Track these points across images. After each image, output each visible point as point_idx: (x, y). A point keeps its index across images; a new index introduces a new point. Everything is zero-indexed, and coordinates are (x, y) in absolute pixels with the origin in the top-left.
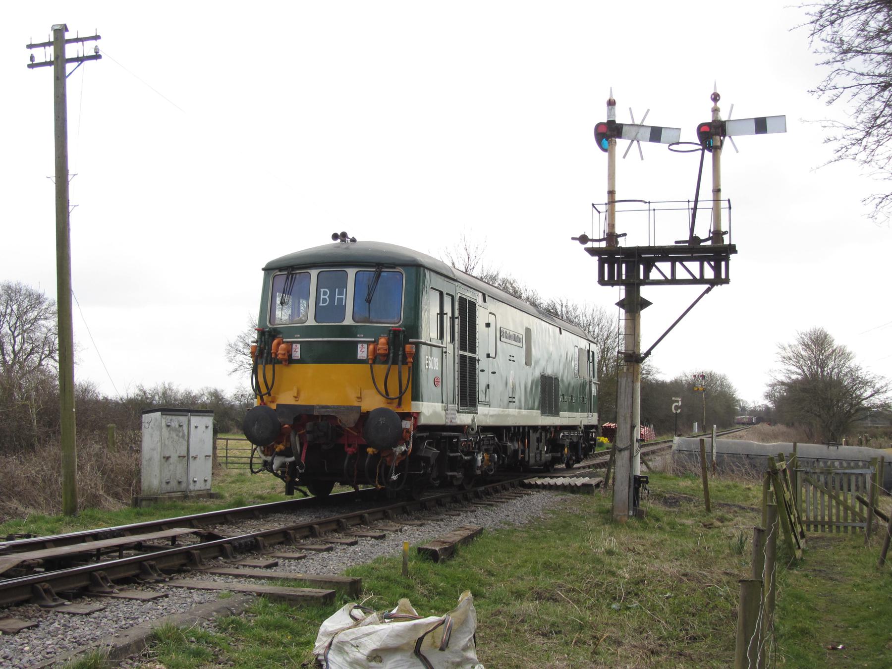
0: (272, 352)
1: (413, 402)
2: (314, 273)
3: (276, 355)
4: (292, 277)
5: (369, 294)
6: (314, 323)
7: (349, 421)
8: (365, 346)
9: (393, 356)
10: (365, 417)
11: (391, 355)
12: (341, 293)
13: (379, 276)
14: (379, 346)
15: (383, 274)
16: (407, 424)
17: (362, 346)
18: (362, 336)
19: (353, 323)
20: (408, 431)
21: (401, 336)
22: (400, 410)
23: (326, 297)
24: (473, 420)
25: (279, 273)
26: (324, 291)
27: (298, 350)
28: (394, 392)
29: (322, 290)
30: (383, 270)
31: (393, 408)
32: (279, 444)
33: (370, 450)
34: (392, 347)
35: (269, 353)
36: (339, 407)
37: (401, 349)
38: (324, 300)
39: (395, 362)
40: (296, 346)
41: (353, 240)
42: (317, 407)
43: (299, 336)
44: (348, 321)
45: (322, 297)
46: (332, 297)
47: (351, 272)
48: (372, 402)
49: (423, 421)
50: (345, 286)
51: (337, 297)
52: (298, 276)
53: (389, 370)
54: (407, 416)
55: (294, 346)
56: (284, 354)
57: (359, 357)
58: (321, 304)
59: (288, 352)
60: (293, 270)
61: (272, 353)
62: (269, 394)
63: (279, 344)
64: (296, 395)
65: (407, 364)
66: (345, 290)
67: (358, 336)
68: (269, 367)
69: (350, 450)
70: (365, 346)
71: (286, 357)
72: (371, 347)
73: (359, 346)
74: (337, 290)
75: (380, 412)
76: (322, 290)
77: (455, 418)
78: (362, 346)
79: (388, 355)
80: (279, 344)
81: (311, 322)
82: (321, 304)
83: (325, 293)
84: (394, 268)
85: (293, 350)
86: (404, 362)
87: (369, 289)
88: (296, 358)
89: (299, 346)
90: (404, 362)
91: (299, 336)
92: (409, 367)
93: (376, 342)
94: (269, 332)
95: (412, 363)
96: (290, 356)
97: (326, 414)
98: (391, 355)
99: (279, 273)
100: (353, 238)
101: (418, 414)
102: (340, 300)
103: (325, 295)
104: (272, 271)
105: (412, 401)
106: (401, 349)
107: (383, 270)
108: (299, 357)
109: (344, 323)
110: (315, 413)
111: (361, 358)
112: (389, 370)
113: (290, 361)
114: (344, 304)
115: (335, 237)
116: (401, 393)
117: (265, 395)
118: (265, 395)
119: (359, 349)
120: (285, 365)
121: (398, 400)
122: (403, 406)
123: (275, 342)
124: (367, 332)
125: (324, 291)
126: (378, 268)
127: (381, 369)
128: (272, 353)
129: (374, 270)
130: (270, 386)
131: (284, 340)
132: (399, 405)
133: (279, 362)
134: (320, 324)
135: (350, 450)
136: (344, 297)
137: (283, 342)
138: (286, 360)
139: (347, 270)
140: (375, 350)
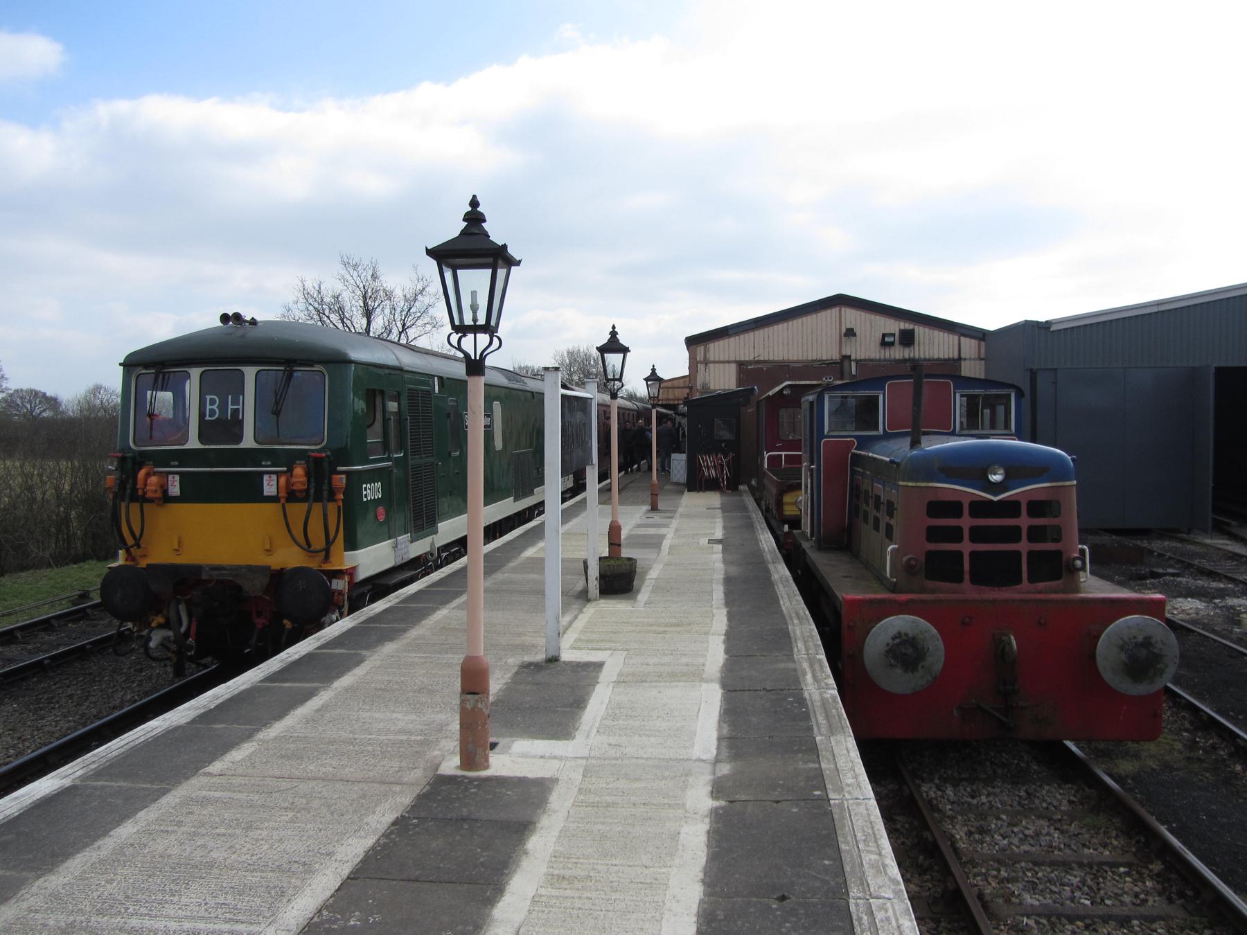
0: (138, 487)
1: (346, 553)
2: (195, 372)
3: (145, 493)
4: (164, 377)
5: (277, 403)
7: (254, 586)
8: (274, 477)
9: (315, 492)
10: (278, 577)
11: (312, 491)
12: (235, 402)
13: (290, 377)
14: (294, 480)
15: (295, 374)
16: (339, 585)
17: (270, 477)
18: (269, 463)
19: (255, 446)
20: (341, 593)
21: (326, 466)
22: (328, 567)
23: (215, 407)
24: (432, 544)
25: (144, 371)
26: (210, 399)
27: (177, 484)
28: (318, 542)
29: (208, 397)
30: (295, 368)
31: (314, 564)
32: (157, 616)
33: (288, 624)
34: (312, 480)
35: (134, 489)
36: (239, 568)
37: (326, 482)
38: (212, 412)
39: (318, 498)
40: (174, 478)
41: (253, 322)
42: (207, 569)
43: (177, 463)
45: (208, 407)
46: (223, 407)
47: (250, 372)
48: (289, 557)
49: (362, 575)
50: (242, 391)
51: (230, 407)
52: (172, 375)
53: (309, 512)
54: (338, 574)
55: (170, 477)
56: (156, 491)
57: (266, 493)
58: (207, 418)
59: (162, 487)
60: (162, 368)
61: (138, 489)
62: (139, 547)
63: (148, 475)
64: (176, 546)
65: (335, 501)
66: (241, 397)
67: (263, 463)
68: (135, 508)
69: (260, 622)
70: (274, 477)
71: (159, 495)
72: (283, 480)
73: (266, 477)
74: (230, 397)
75: (299, 571)
76: (208, 397)
77: (408, 552)
78: (270, 477)
79: (308, 490)
80: (148, 475)
81: (194, 443)
82: (207, 418)
83: (213, 402)
84: (312, 366)
85: (170, 483)
86: (332, 498)
87: (276, 395)
88: (174, 494)
89: (177, 478)
90: (332, 498)
91: (177, 463)
92: (339, 507)
93: (290, 470)
94: (134, 459)
95: (343, 500)
96: (165, 492)
97: (221, 578)
98: (312, 491)
99: (144, 371)
100: (253, 318)
101: (354, 568)
102: (236, 412)
103: (213, 406)
105: (345, 551)
106: (326, 482)
107: (295, 368)
108: (178, 493)
109: (242, 446)
110: (204, 577)
111: (270, 494)
112: (309, 512)
113: (166, 499)
114: (240, 417)
115: (225, 318)
116: (329, 543)
117: (132, 547)
118: (132, 547)
119: (265, 483)
120: (158, 505)
121: (324, 553)
122: (332, 559)
123: (142, 473)
124: (275, 457)
125: (210, 399)
126: (288, 367)
127: (297, 510)
128: (138, 489)
129: (283, 368)
130: (138, 535)
131: (156, 469)
132: (327, 558)
133: (151, 501)
134: (207, 447)
135: (260, 622)
136: (240, 407)
137: (155, 473)
138: (159, 499)
139: (245, 369)
140: (288, 482)
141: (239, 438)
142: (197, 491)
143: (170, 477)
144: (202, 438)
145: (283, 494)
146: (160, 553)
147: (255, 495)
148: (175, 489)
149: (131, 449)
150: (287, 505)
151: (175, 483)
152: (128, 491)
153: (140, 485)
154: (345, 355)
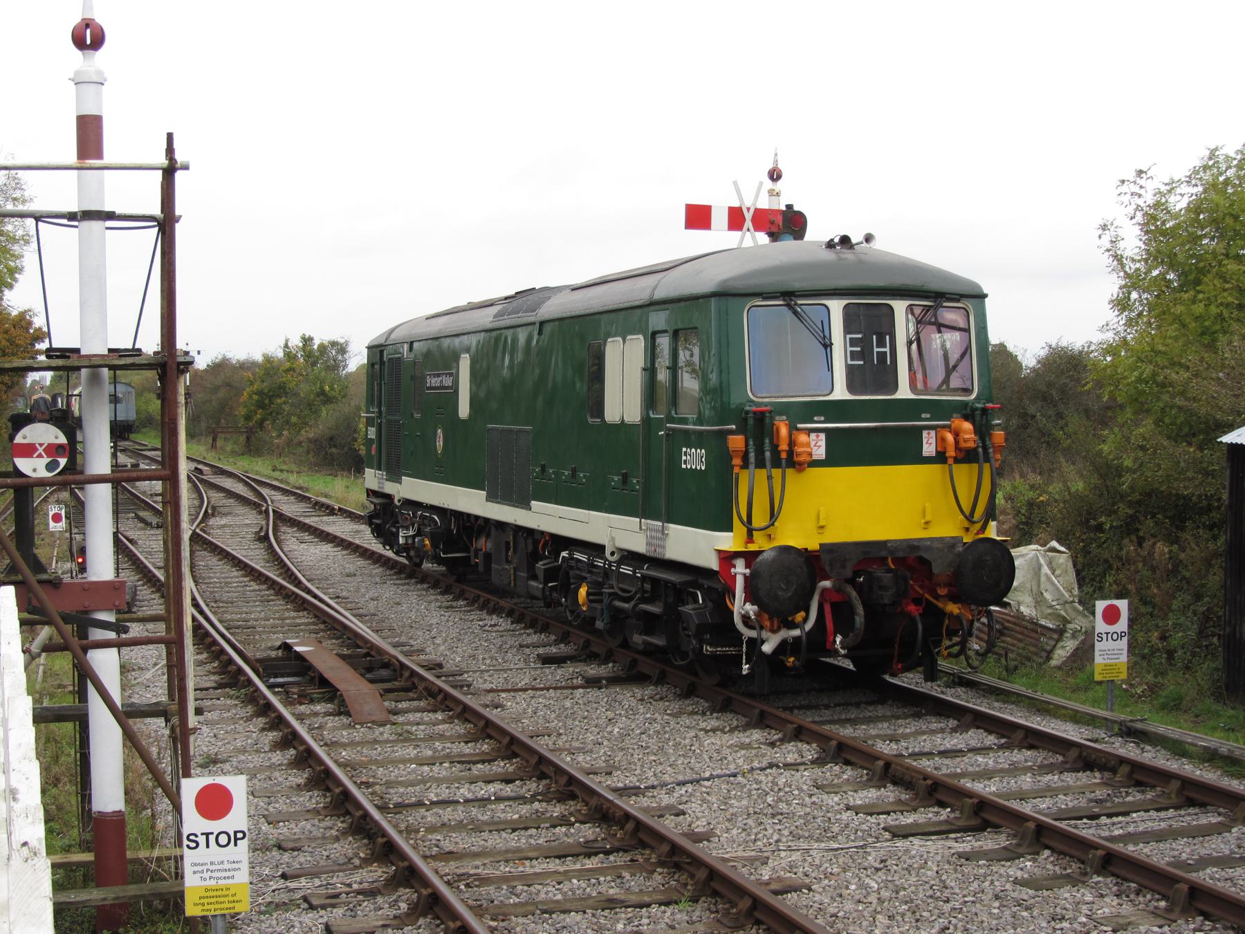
6: (848, 396)
8: (933, 433)
12: (881, 343)
17: (929, 434)
27: (823, 443)
43: (822, 419)
44: (904, 392)
51: (876, 350)
57: (925, 454)
61: (779, 452)
70: (933, 433)
73: (925, 433)
76: (848, 336)
81: (840, 392)
84: (958, 301)
89: (822, 436)
90: (987, 460)
102: (882, 356)
104: (747, 299)
107: (945, 304)
108: (823, 457)
119: (925, 441)
124: (939, 410)
127: (964, 475)
136: (887, 350)
141: (895, 387)
143: (813, 436)
144: (851, 387)
145: (951, 453)
148: (820, 452)
149: (752, 401)
150: (954, 466)
151: (819, 444)
152: (768, 454)
153: (784, 446)
154: (979, 287)
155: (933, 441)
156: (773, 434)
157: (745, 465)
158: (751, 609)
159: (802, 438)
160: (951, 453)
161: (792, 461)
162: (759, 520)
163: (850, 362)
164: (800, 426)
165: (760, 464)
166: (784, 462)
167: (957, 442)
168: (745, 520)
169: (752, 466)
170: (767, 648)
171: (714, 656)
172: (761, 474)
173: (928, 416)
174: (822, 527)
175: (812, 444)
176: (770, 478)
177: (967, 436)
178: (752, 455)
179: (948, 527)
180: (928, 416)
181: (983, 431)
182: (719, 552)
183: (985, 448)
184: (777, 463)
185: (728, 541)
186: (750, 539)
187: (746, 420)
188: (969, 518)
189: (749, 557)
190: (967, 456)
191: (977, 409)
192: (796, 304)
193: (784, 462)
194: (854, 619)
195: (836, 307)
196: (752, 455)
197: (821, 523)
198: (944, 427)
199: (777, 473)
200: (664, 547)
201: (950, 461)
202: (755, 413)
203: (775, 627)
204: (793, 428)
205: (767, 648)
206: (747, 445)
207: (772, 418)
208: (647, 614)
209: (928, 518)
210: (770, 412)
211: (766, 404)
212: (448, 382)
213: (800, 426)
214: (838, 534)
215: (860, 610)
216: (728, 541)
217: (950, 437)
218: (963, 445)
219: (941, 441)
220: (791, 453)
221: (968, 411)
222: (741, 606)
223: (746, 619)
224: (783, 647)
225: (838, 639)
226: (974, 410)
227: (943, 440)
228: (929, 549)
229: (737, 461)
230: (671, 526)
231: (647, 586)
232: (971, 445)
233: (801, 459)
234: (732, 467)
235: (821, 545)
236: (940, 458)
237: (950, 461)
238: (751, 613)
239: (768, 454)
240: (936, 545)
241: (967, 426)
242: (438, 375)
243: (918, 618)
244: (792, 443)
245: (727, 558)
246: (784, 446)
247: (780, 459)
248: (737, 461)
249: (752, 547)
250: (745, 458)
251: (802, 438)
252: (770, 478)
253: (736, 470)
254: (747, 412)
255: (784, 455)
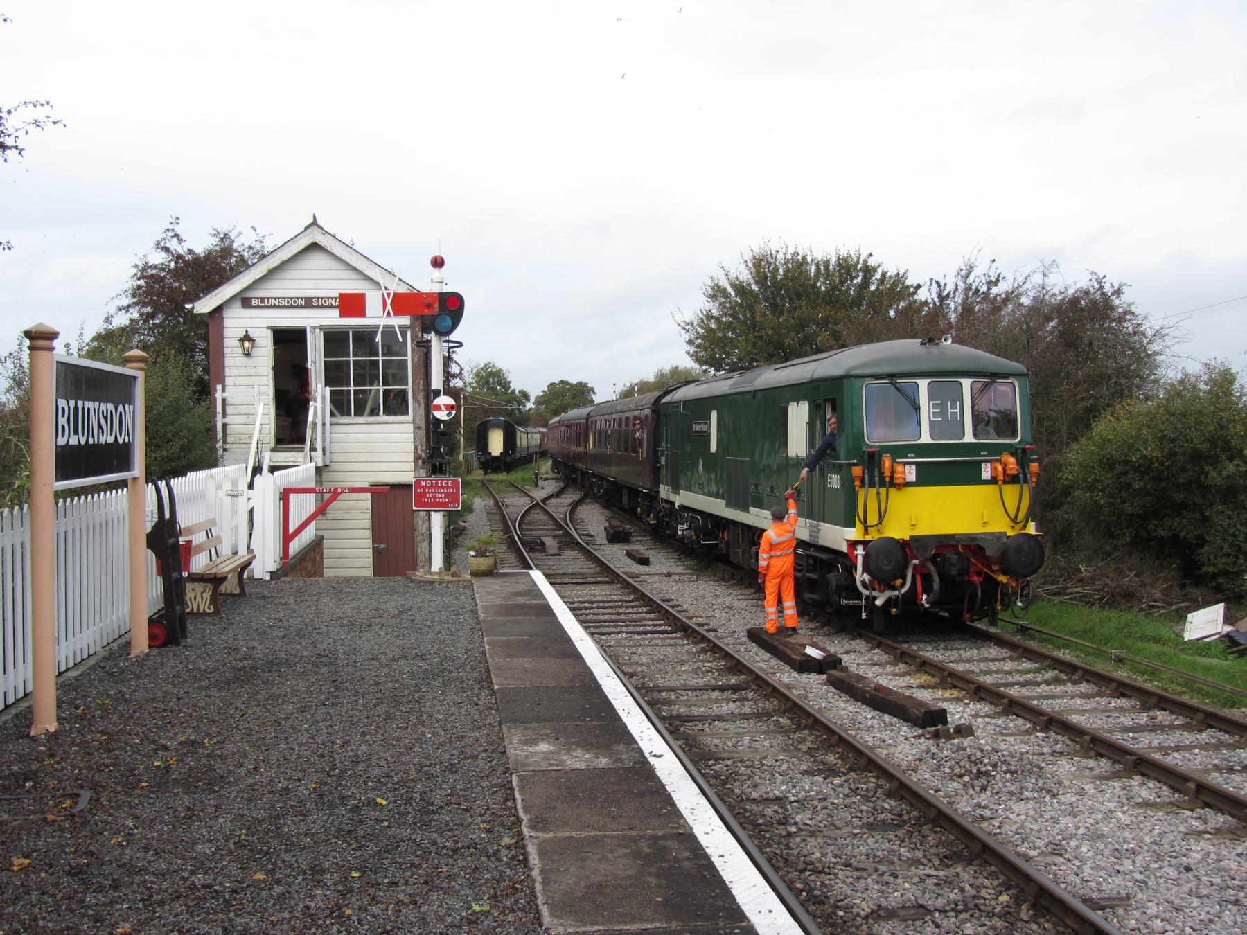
6: (930, 441)
8: (989, 465)
44: (969, 438)
47: (966, 383)
51: (950, 411)
57: (983, 478)
61: (884, 478)
67: (982, 453)
70: (989, 465)
76: (931, 403)
81: (926, 439)
84: (1007, 378)
89: (914, 467)
90: (1026, 481)
108: (914, 480)
119: (983, 470)
127: (1011, 492)
136: (958, 411)
142: (929, 476)
145: (1000, 477)
146: (897, 530)
147: (976, 479)
150: (1004, 487)
152: (877, 478)
153: (887, 474)
155: (989, 469)
156: (880, 466)
157: (862, 486)
158: (866, 577)
159: (899, 468)
160: (1000, 477)
161: (893, 483)
162: (872, 519)
163: (932, 419)
164: (898, 460)
165: (872, 485)
166: (887, 484)
167: (1004, 470)
168: (862, 519)
169: (866, 486)
170: (878, 602)
171: (847, 606)
172: (873, 491)
173: (986, 453)
174: (913, 525)
175: (907, 472)
176: (878, 493)
177: (1011, 467)
178: (866, 479)
179: (1000, 525)
180: (986, 453)
181: (1023, 462)
182: (847, 540)
183: (1025, 475)
184: (882, 484)
185: (854, 533)
186: (866, 532)
187: (863, 457)
188: (1015, 521)
189: (865, 543)
190: (1013, 480)
191: (1018, 449)
192: (896, 382)
193: (887, 484)
194: (932, 585)
195: (923, 383)
196: (866, 479)
197: (913, 523)
198: (996, 460)
199: (883, 490)
200: (818, 537)
201: (1000, 483)
202: (869, 452)
203: (882, 589)
204: (893, 461)
205: (878, 602)
206: (863, 472)
207: (880, 457)
208: (810, 579)
209: (985, 520)
210: (879, 452)
211: (876, 447)
212: (705, 428)
213: (898, 460)
214: (921, 531)
215: (936, 578)
216: (854, 533)
217: (1000, 468)
218: (1008, 472)
219: (994, 469)
220: (892, 477)
221: (1013, 450)
222: (861, 576)
223: (863, 583)
224: (889, 602)
225: (924, 597)
226: (1016, 449)
227: (996, 469)
228: (984, 539)
229: (857, 483)
230: (822, 524)
231: (811, 562)
232: (1014, 472)
233: (899, 481)
234: (854, 487)
235: (910, 537)
236: (993, 480)
237: (1000, 483)
238: (867, 580)
239: (877, 478)
240: (987, 537)
241: (1012, 460)
242: (700, 424)
243: (979, 585)
244: (893, 472)
245: (853, 544)
246: (887, 474)
247: (885, 482)
248: (857, 483)
249: (868, 538)
250: (862, 481)
251: (899, 468)
252: (878, 493)
253: (857, 488)
254: (864, 452)
255: (887, 479)
